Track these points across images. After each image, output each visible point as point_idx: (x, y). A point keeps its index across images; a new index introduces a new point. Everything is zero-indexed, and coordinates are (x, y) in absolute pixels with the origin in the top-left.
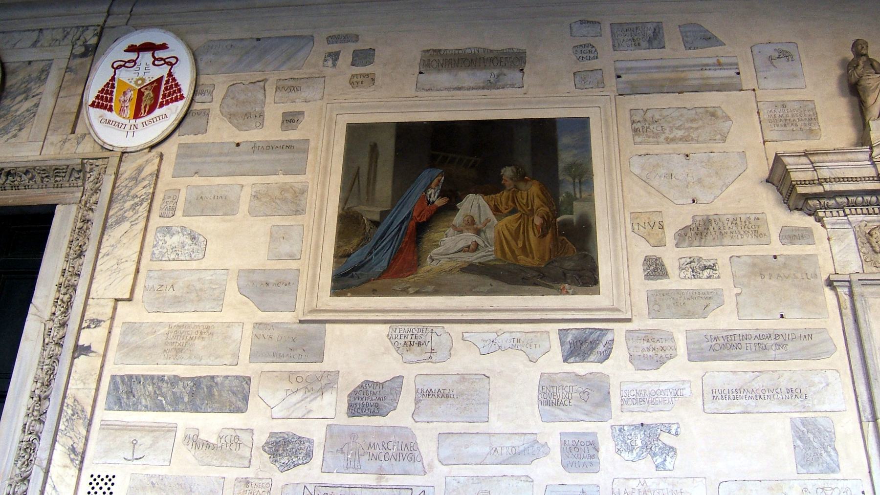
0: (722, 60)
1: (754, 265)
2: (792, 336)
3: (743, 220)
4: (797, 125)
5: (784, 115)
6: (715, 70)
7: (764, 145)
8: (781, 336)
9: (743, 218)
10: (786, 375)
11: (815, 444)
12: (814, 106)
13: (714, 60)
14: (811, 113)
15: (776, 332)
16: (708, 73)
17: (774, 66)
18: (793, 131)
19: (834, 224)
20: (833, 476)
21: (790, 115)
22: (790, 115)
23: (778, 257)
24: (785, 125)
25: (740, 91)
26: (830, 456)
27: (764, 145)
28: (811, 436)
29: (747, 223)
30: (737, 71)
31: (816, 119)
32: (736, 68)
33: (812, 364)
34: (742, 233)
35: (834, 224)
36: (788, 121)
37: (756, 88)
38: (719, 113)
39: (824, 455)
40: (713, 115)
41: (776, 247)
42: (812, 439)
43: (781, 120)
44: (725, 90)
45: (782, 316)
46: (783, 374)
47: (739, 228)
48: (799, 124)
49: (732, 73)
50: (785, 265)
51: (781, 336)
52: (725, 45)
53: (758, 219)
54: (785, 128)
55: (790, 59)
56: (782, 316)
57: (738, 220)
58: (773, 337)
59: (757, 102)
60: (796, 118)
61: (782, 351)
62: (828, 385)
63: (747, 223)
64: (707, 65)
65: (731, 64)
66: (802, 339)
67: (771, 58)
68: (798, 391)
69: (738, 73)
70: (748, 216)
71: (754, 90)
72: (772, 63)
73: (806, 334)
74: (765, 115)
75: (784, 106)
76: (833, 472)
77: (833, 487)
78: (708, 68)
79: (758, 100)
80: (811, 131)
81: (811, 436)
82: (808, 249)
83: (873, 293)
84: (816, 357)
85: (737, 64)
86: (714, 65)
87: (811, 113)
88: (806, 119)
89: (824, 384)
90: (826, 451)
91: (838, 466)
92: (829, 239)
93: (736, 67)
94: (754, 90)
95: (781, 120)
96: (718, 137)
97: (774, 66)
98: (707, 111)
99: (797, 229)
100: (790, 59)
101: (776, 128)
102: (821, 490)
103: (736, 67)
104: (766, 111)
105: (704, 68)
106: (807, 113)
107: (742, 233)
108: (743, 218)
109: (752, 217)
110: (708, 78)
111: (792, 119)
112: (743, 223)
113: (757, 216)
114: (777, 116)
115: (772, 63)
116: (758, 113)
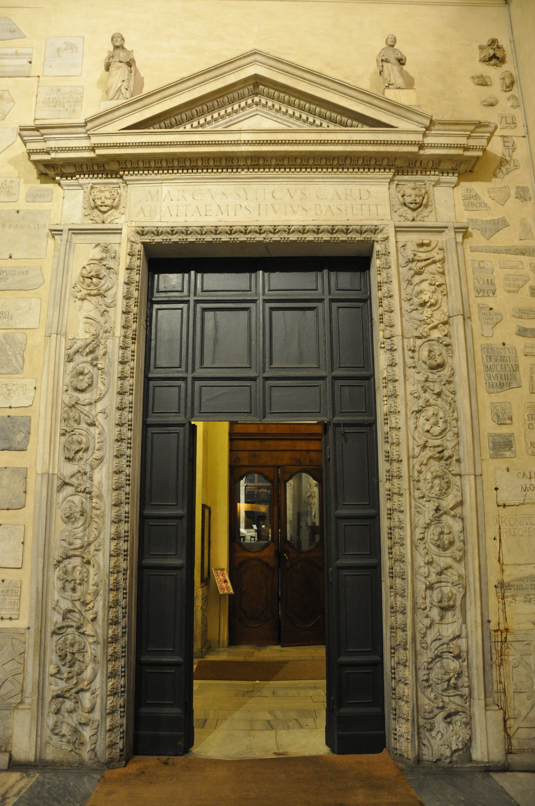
0: (20, 51)
4: (64, 106)
5: (57, 98)
6: (12, 59)
8: (5, 272)
11: (9, 353)
13: (13, 51)
14: (79, 96)
17: (60, 56)
18: (60, 111)
20: (18, 376)
26: (17, 361)
28: (8, 347)
29: (4, 184)
30: (30, 60)
37: (41, 76)
39: (14, 360)
41: (22, 204)
42: (8, 349)
49: (25, 62)
51: (5, 272)
55: (75, 51)
59: (38, 86)
62: (30, 309)
63: (4, 184)
64: (6, 54)
65: (25, 54)
67: (59, 50)
68: (7, 313)
69: (30, 63)
70: (5, 179)
72: (59, 54)
73: (24, 271)
74: (41, 99)
75: (59, 90)
76: (17, 373)
77: (14, 383)
78: (6, 57)
80: (74, 111)
81: (8, 347)
82: (46, 206)
85: (31, 54)
86: (13, 54)
87: (79, 96)
88: (73, 101)
90: (16, 358)
91: (22, 369)
92: (63, 198)
93: (29, 56)
94: (39, 77)
97: (60, 56)
100: (75, 51)
102: (5, 386)
103: (29, 56)
105: (3, 57)
109: (9, 180)
110: (5, 66)
111: (62, 101)
114: (51, 98)
115: (59, 54)
116: (37, 96)
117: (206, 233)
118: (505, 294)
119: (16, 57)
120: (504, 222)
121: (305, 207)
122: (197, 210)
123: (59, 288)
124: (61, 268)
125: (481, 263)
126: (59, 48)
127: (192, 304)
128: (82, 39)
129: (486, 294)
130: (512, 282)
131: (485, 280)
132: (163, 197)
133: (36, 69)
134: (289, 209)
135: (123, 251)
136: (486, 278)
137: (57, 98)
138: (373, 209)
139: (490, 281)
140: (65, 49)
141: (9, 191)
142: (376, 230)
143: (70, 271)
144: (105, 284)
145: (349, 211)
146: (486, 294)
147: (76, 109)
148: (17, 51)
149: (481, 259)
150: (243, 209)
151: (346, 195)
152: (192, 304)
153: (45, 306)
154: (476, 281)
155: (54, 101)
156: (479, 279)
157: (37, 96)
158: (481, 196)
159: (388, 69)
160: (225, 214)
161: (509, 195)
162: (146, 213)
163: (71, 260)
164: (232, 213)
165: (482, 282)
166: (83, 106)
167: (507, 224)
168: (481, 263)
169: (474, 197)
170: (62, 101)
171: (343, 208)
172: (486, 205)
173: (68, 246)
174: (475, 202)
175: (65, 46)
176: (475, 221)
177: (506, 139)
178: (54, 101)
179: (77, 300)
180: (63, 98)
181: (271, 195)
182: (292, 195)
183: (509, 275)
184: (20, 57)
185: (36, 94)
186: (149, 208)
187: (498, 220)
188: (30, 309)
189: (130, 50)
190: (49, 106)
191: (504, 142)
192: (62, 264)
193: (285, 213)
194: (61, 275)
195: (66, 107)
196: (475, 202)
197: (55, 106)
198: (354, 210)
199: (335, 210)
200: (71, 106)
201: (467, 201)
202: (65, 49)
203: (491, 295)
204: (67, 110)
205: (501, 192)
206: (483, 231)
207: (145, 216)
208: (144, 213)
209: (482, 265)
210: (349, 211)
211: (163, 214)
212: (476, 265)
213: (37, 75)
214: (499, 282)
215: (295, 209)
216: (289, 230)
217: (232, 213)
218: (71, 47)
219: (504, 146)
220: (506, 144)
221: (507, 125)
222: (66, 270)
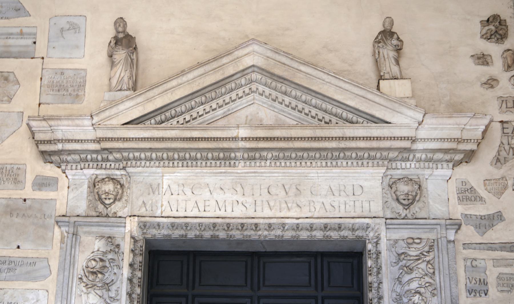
0: (25, 30)
1: (7, 206)
2: (23, 262)
3: (8, 169)
4: (67, 91)
5: (61, 82)
7: (39, 106)
8: (13, 263)
9: (9, 167)
10: (10, 292)
12: (85, 75)
13: (18, 30)
14: (82, 80)
15: (12, 259)
16: (11, 42)
17: (63, 37)
18: (64, 95)
19: (74, 175)
21: (65, 81)
22: (65, 81)
23: (27, 201)
24: (59, 91)
25: (32, 58)
27: (39, 106)
29: (11, 171)
30: (34, 40)
31: (84, 86)
32: (34, 38)
33: (31, 285)
34: (5, 179)
35: (74, 175)
36: (62, 87)
37: (45, 57)
38: (11, 77)
40: (6, 79)
43: (57, 86)
44: (21, 58)
45: (18, 247)
46: (8, 291)
47: (4, 175)
48: (70, 90)
49: (30, 42)
50: (30, 208)
51: (13, 263)
52: (30, 16)
53: (19, 169)
54: (58, 93)
55: (77, 31)
56: (18, 247)
57: (4, 171)
58: (7, 263)
59: (42, 69)
60: (69, 85)
61: (12, 273)
62: (37, 301)
63: (11, 171)
64: (12, 34)
65: (30, 34)
66: (28, 265)
67: (62, 30)
69: (35, 43)
70: (12, 166)
71: (43, 58)
72: (62, 34)
73: (32, 262)
74: (45, 81)
75: (62, 73)
78: (11, 37)
79: (44, 67)
80: (77, 95)
83: (85, 233)
84: (35, 279)
85: (35, 34)
86: (17, 34)
87: (82, 80)
89: (35, 300)
92: (68, 187)
93: (34, 36)
95: (57, 86)
96: (6, 98)
97: (63, 37)
98: (2, 76)
99: (47, 178)
100: (77, 31)
101: (51, 93)
103: (34, 36)
104: (47, 77)
105: (9, 37)
106: (78, 80)
107: (5, 179)
108: (9, 167)
109: (15, 167)
110: (10, 46)
111: (66, 85)
112: (8, 172)
113: (19, 166)
114: (55, 82)
115: (62, 34)
116: (41, 79)
117: (204, 229)
118: (498, 294)
119: (21, 37)
120: (499, 217)
121: (299, 204)
122: (196, 205)
123: (66, 281)
124: (68, 261)
125: (474, 261)
126: (62, 28)
127: (190, 298)
128: (85, 18)
129: (478, 295)
130: (505, 282)
131: (478, 280)
132: (164, 190)
133: (41, 49)
134: (284, 205)
135: (126, 246)
136: (478, 278)
137: (61, 82)
138: (366, 205)
139: (482, 281)
140: (69, 30)
141: (15, 179)
142: (367, 228)
143: (76, 265)
144: (109, 277)
145: (342, 207)
146: (478, 295)
147: (79, 94)
148: (21, 30)
149: (473, 256)
150: (240, 204)
151: (340, 191)
152: (190, 298)
153: (52, 298)
154: (468, 281)
155: (58, 84)
156: (471, 278)
157: (41, 79)
158: (477, 189)
159: (384, 56)
160: (223, 209)
161: (505, 188)
162: (147, 207)
163: (77, 253)
164: (229, 209)
165: (474, 281)
166: (86, 91)
167: (503, 219)
168: (474, 261)
169: (469, 191)
170: (66, 85)
171: (336, 204)
172: (481, 199)
173: (74, 239)
174: (470, 195)
175: (67, 26)
176: (469, 216)
177: (505, 125)
178: (58, 84)
179: (82, 294)
180: (67, 81)
181: (266, 191)
182: (287, 190)
183: (503, 274)
184: (25, 36)
186: (150, 202)
187: (493, 214)
188: (37, 301)
189: (133, 37)
190: (53, 90)
191: (503, 128)
192: (69, 257)
193: (280, 209)
194: (68, 268)
195: (69, 91)
196: (470, 195)
197: (59, 91)
198: (347, 206)
199: (328, 207)
200: (74, 91)
201: (462, 195)
202: (69, 30)
203: (483, 295)
204: (70, 95)
205: (498, 184)
206: (477, 227)
207: (147, 210)
208: (145, 207)
209: (474, 263)
210: (342, 207)
211: (163, 208)
212: (469, 263)
213: (41, 56)
214: (492, 280)
215: (289, 205)
216: (284, 227)
217: (229, 209)
218: (74, 28)
219: (503, 133)
220: (506, 131)
221: (508, 109)
222: (72, 264)
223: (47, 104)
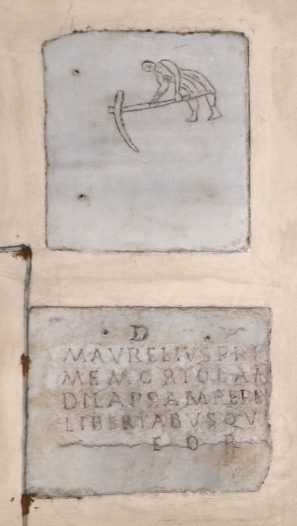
5: (134, 376)
7: (26, 511)
12: (262, 338)
14: (247, 368)
17: (128, 141)
18: (156, 447)
27: (26, 511)
36: (142, 404)
43: (114, 399)
54: (123, 437)
59: (29, 309)
60: (180, 390)
72: (120, 126)
79: (34, 300)
87: (247, 368)
88: (219, 394)
95: (114, 399)
97: (128, 141)
104: (57, 352)
111: (162, 393)
114: (103, 376)
115: (120, 126)
116: (26, 361)
137: (134, 376)
147: (239, 437)
155: (122, 390)
157: (26, 361)
166: (276, 421)
170: (162, 393)
178: (122, 390)
180: (169, 375)
185: (20, 351)
195: (186, 427)
223: (69, 496)
